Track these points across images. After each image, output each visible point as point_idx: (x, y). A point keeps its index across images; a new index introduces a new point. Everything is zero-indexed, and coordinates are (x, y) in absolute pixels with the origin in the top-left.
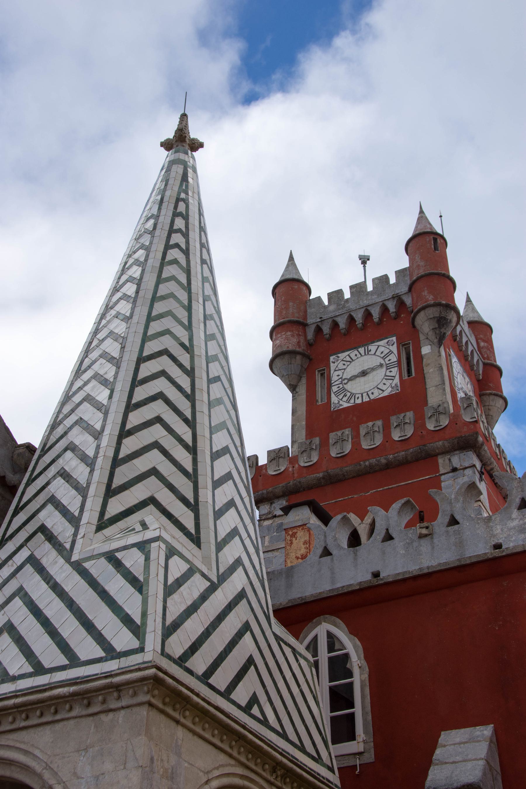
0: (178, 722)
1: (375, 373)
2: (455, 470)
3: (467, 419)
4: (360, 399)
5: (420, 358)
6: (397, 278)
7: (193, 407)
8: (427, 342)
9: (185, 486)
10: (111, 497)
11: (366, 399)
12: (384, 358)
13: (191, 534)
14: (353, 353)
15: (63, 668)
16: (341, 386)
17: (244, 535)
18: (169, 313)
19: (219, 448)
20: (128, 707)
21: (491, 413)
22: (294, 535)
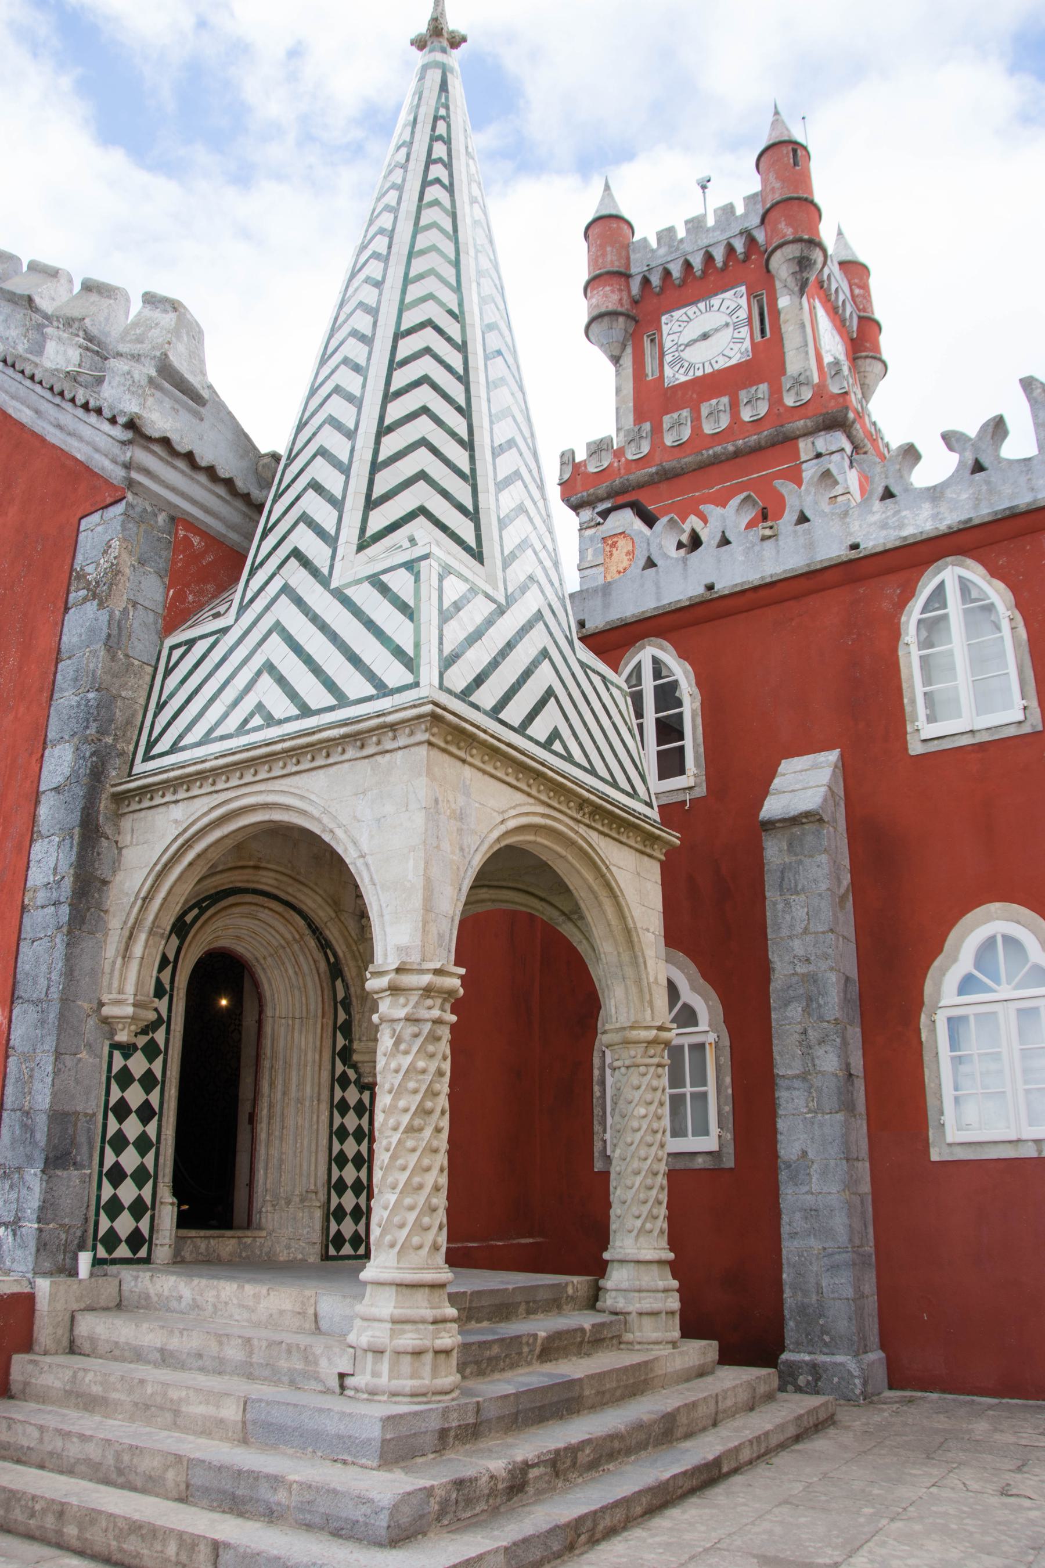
0: (464, 761)
1: (719, 335)
2: (819, 456)
3: (835, 390)
4: (701, 369)
5: (776, 313)
6: (746, 206)
7: (468, 391)
8: (785, 291)
9: (462, 492)
10: (373, 509)
11: (709, 370)
12: (730, 315)
13: (472, 548)
14: (691, 310)
15: (331, 709)
16: (676, 354)
17: (538, 547)
18: (432, 272)
19: (503, 441)
20: (405, 747)
21: (867, 381)
22: (614, 545)
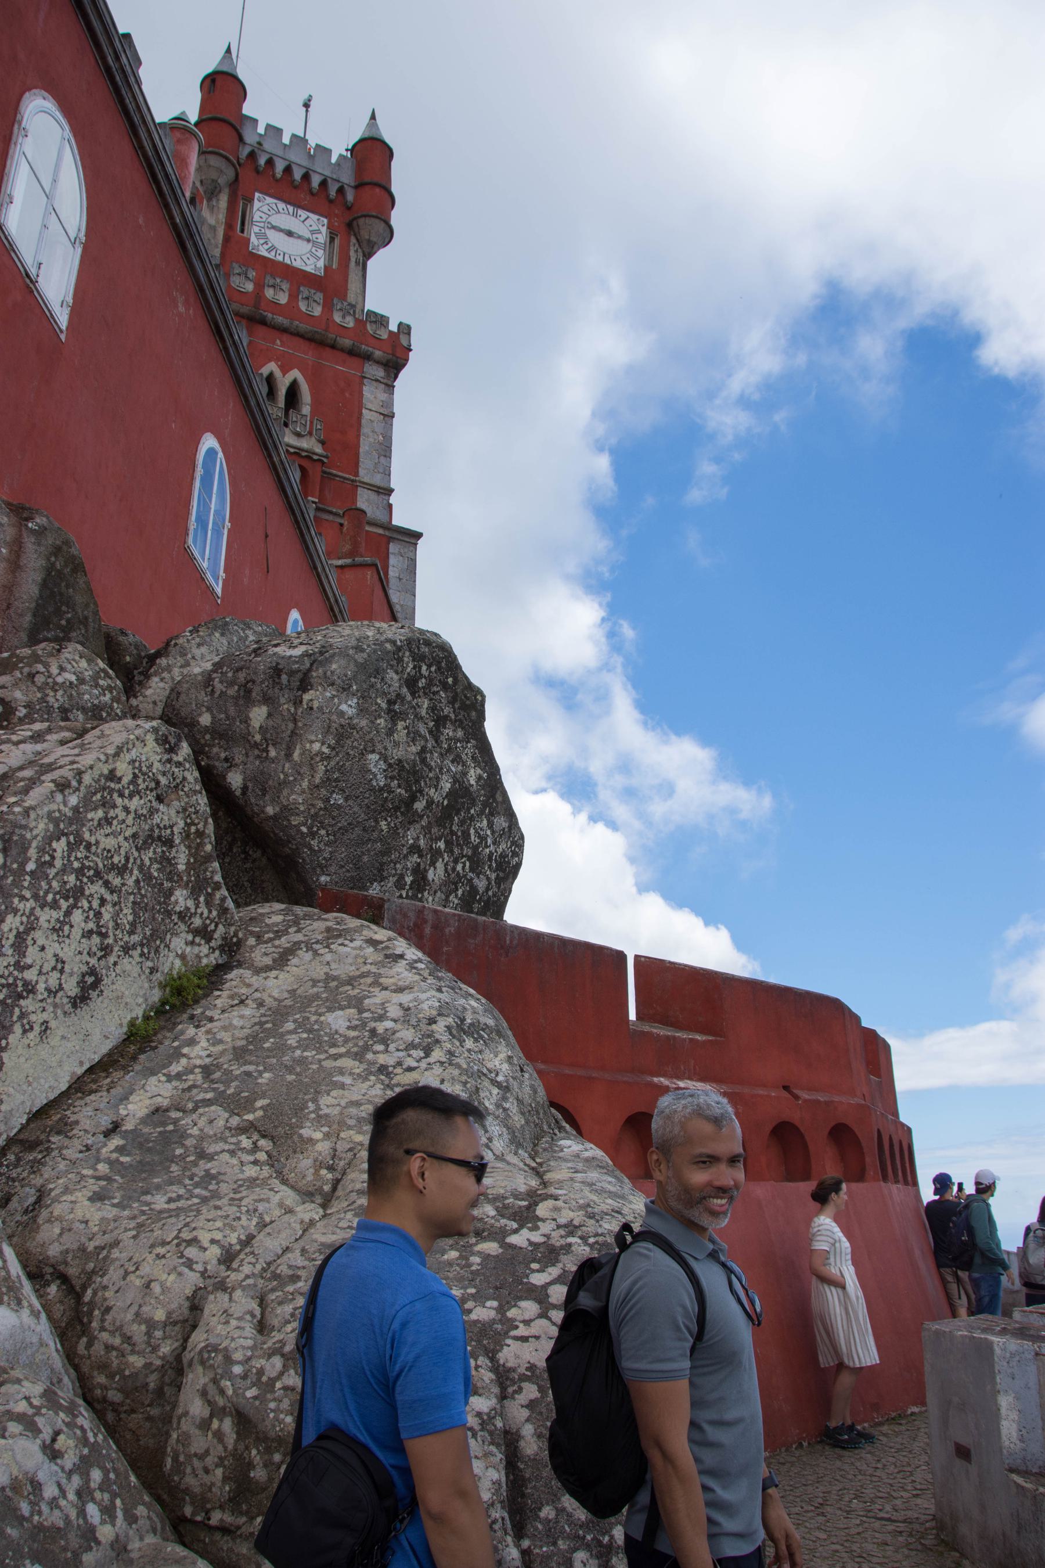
1: (300, 241)
14: (281, 205)
